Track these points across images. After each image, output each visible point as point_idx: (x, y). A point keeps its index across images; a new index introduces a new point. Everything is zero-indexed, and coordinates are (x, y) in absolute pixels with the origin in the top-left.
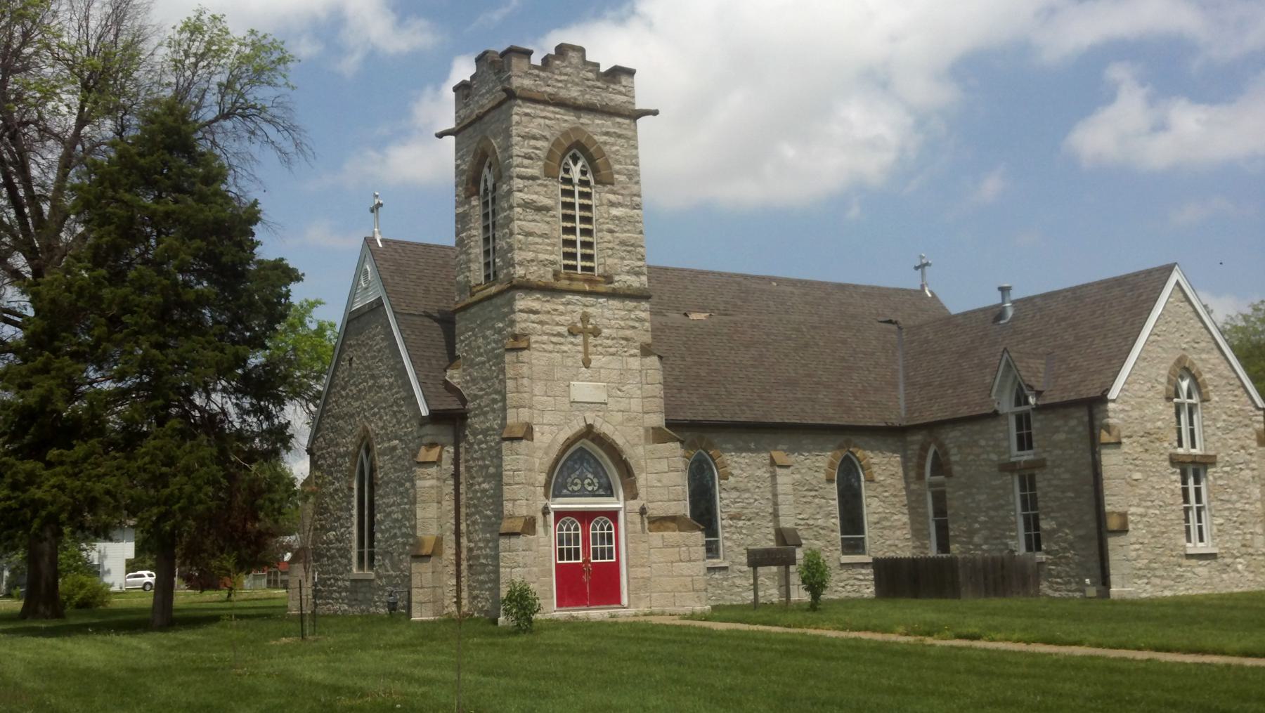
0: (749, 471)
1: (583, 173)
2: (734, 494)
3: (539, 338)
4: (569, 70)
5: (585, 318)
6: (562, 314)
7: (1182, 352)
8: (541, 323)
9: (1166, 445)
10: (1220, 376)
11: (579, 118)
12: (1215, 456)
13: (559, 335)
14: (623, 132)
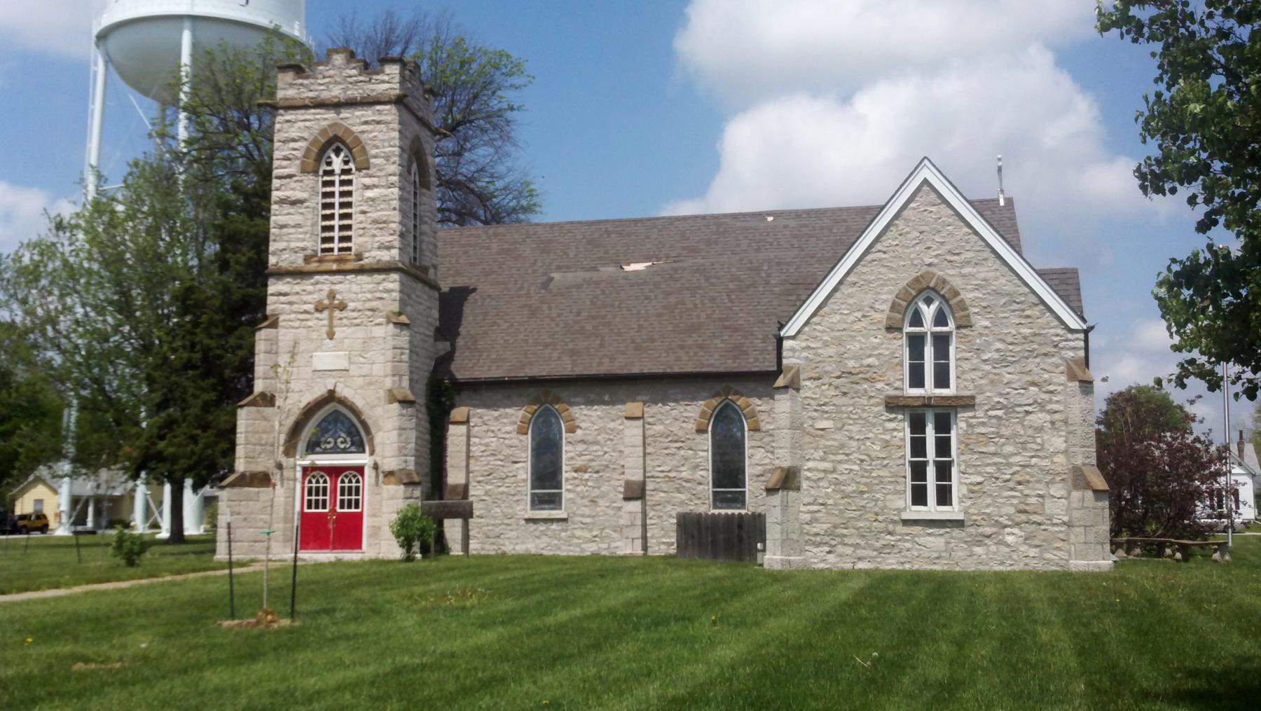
0: (600, 424)
1: (346, 163)
2: (581, 447)
3: (287, 317)
4: (332, 72)
5: (332, 295)
6: (310, 293)
7: (925, 269)
8: (291, 303)
9: (879, 385)
10: (998, 293)
11: (338, 114)
12: (973, 398)
13: (306, 312)
14: (383, 118)
